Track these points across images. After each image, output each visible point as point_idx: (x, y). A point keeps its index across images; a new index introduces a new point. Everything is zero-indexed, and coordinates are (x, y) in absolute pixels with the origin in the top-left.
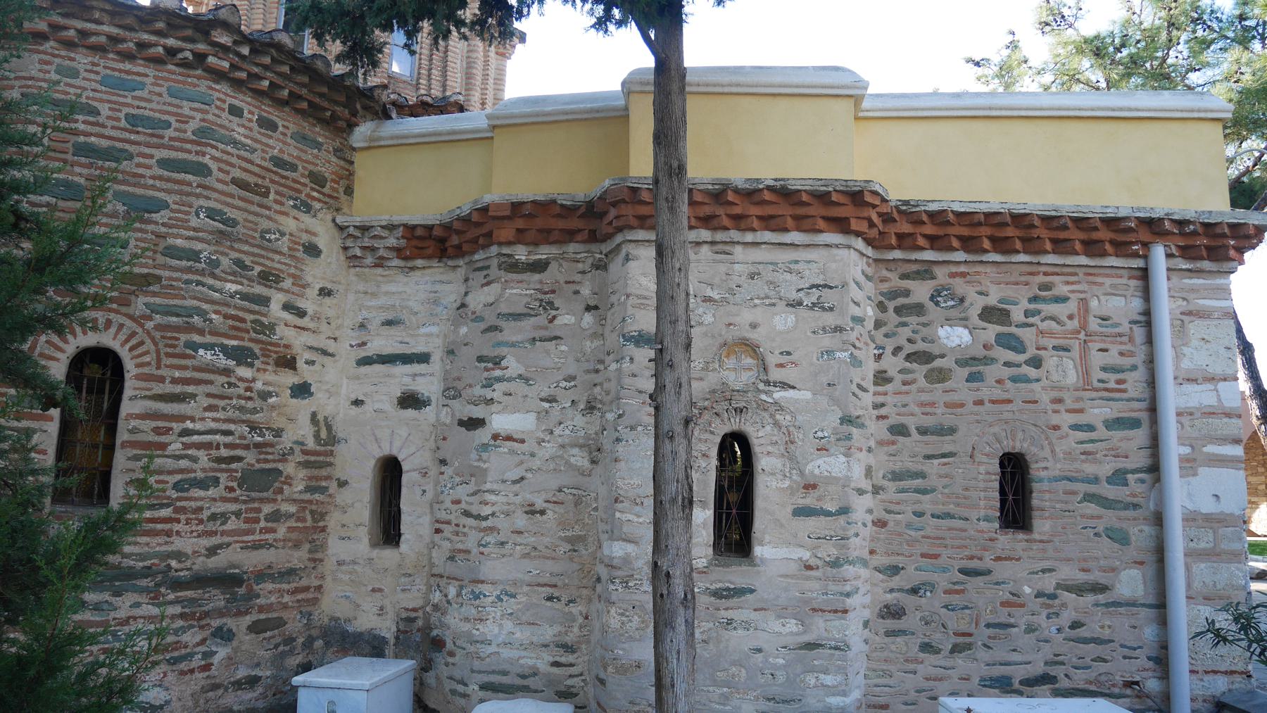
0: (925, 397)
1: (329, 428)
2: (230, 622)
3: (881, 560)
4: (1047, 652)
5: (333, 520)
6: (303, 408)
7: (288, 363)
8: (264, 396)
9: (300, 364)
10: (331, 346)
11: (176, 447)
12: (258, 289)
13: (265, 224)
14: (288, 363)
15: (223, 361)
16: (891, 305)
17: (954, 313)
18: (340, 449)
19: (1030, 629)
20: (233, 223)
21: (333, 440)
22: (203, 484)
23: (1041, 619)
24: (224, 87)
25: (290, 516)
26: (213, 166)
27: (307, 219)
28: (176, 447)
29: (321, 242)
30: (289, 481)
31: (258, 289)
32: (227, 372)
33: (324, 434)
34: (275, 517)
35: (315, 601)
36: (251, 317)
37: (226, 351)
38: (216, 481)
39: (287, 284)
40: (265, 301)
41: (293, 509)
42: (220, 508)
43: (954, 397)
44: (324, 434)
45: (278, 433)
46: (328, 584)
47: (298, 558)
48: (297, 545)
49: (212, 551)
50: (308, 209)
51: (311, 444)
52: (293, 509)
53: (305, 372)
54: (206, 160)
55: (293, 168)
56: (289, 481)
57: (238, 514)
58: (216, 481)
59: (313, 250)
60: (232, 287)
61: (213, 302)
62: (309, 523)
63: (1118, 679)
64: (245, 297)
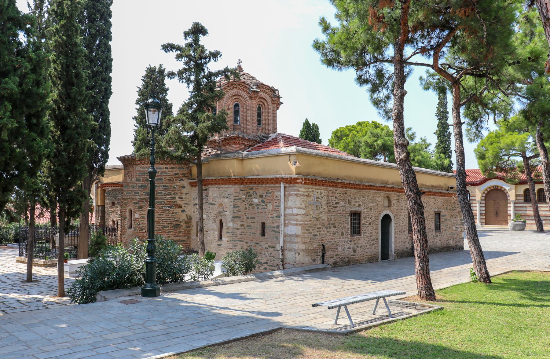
0: (251, 212)
1: (190, 217)
4: (267, 258)
5: (192, 232)
6: (184, 214)
7: (181, 207)
8: (176, 213)
9: (182, 207)
10: (189, 203)
11: (161, 222)
13: (174, 185)
14: (181, 207)
15: (168, 208)
16: (247, 195)
17: (255, 196)
18: (192, 220)
20: (168, 186)
21: (191, 218)
23: (266, 253)
24: (164, 165)
25: (182, 232)
26: (163, 178)
27: (182, 182)
28: (161, 222)
29: (185, 185)
30: (182, 226)
32: (168, 210)
33: (189, 218)
34: (180, 232)
35: (189, 245)
36: (172, 201)
37: (168, 207)
38: (168, 227)
39: (179, 194)
40: (175, 198)
41: (183, 230)
42: (169, 231)
43: (255, 212)
44: (189, 218)
45: (179, 218)
46: (191, 242)
47: (185, 238)
48: (185, 236)
50: (182, 180)
51: (186, 219)
52: (183, 230)
53: (184, 208)
54: (162, 178)
55: (178, 174)
56: (182, 226)
57: (173, 231)
58: (168, 227)
59: (184, 187)
60: (168, 197)
61: (165, 200)
62: (187, 232)
63: (276, 264)
64: (170, 198)
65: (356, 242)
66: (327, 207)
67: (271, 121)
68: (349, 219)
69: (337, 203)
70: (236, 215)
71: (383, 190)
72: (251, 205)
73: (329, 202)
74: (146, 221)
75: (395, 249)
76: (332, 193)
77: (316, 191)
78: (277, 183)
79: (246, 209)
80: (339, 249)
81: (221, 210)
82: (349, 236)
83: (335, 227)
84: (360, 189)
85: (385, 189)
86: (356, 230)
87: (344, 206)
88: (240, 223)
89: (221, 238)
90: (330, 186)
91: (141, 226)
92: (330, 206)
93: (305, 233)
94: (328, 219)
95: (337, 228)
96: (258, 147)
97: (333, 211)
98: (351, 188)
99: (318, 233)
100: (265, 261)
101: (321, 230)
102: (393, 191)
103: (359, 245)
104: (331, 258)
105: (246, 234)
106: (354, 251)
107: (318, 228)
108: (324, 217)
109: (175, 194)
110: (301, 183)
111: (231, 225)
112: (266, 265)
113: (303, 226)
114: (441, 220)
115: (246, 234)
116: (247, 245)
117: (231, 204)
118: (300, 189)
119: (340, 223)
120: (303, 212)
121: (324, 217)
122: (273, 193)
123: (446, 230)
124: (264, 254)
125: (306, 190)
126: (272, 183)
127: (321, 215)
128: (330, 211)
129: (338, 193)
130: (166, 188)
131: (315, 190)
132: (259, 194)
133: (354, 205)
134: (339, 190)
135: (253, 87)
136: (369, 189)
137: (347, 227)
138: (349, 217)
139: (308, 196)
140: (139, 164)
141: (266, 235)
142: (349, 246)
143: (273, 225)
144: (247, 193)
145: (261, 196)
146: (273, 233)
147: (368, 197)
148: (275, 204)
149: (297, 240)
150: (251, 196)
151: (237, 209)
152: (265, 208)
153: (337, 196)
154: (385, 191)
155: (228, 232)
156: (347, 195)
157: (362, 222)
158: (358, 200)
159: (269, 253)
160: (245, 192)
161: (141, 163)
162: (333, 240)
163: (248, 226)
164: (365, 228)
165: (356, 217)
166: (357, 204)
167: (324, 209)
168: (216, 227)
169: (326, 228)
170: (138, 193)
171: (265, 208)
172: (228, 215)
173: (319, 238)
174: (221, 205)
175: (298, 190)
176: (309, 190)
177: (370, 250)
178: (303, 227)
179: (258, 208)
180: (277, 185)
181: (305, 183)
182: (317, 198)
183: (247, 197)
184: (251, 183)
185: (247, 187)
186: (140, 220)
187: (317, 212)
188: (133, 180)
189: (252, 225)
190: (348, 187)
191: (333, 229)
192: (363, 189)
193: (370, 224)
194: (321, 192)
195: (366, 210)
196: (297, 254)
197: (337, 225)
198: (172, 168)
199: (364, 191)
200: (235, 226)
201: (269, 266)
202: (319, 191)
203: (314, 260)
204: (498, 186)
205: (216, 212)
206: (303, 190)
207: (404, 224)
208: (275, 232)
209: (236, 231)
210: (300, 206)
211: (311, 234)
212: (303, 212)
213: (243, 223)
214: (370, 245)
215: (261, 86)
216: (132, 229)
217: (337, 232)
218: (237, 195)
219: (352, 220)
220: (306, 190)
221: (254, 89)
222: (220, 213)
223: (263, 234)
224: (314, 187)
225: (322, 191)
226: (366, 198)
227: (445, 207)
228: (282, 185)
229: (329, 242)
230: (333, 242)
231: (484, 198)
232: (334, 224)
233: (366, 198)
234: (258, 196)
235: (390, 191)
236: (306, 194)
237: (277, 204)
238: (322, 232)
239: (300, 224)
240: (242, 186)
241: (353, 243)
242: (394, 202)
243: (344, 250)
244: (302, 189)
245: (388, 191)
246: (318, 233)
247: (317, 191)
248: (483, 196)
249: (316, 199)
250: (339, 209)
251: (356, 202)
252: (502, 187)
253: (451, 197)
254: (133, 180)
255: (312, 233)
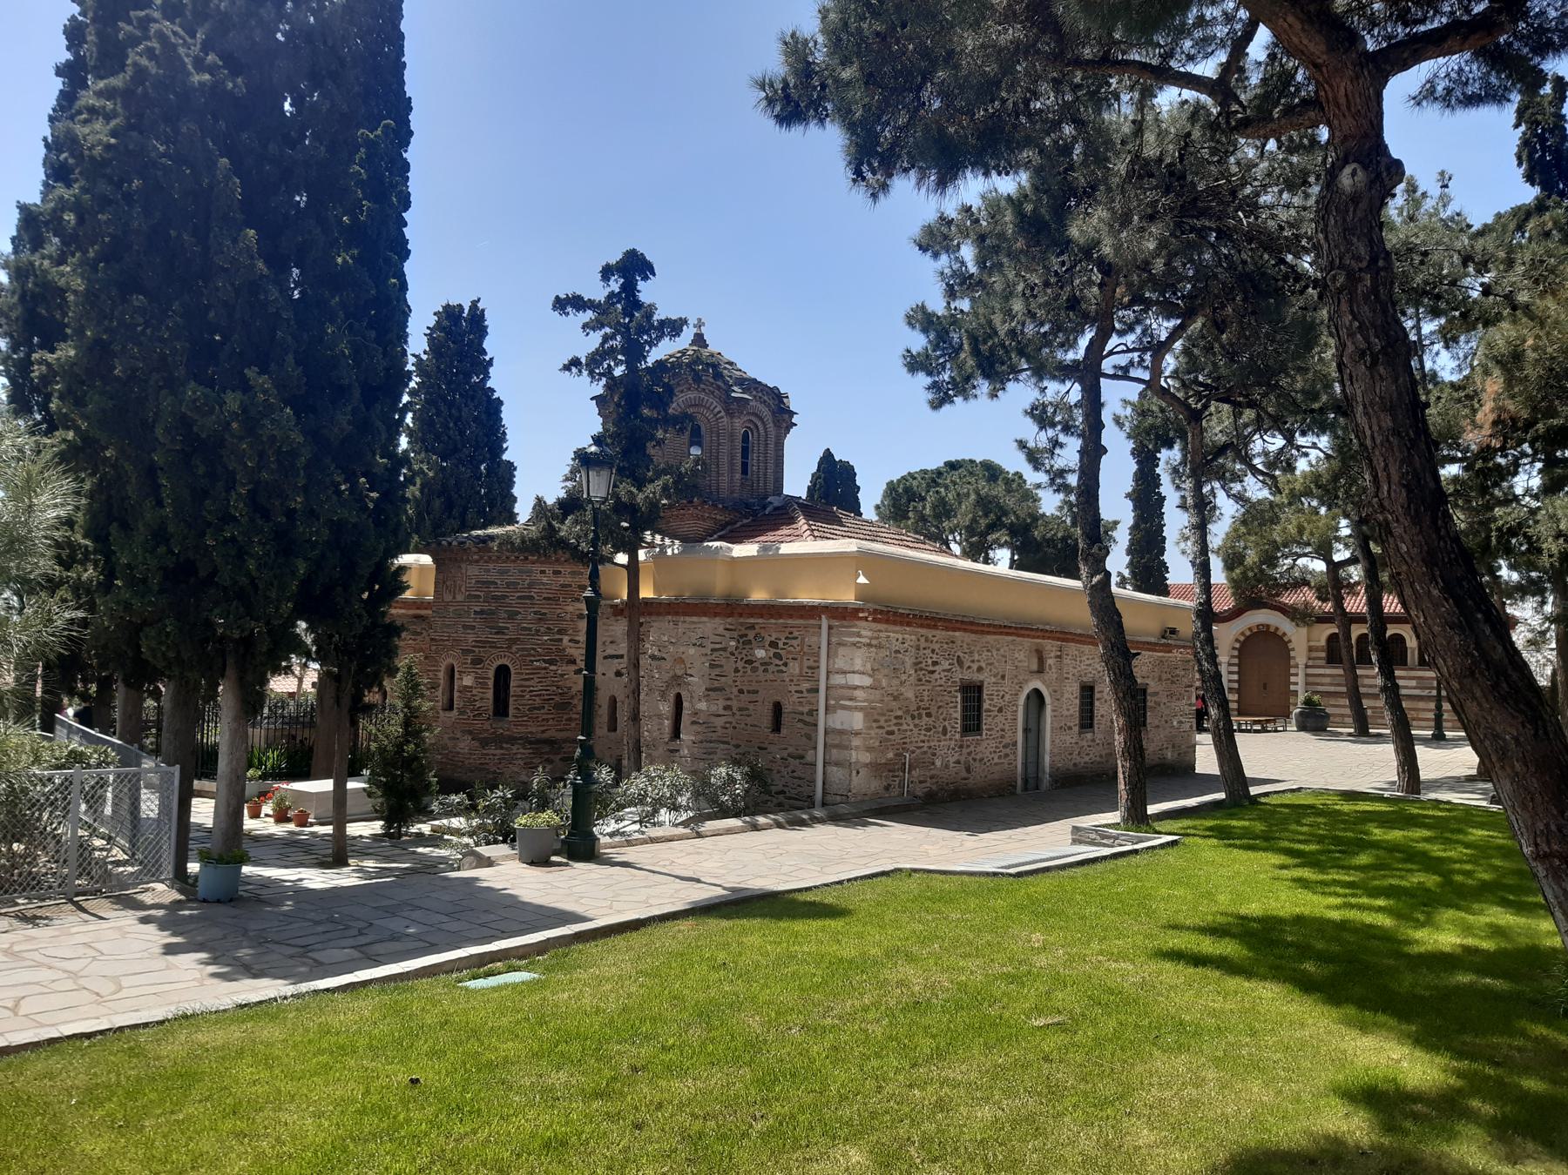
2: (552, 757)
3: (734, 742)
7: (574, 662)
8: (562, 675)
12: (558, 637)
14: (574, 662)
19: (779, 772)
20: (545, 614)
22: (538, 709)
30: (575, 706)
31: (558, 637)
32: (545, 668)
34: (570, 719)
37: (544, 661)
40: (561, 640)
45: (570, 688)
49: (543, 732)
56: (575, 706)
65: (972, 748)
67: (771, 465)
68: (959, 699)
69: (935, 663)
70: (716, 684)
71: (1028, 636)
72: (749, 662)
74: (490, 694)
75: (1051, 767)
76: (926, 640)
77: (896, 636)
78: (812, 617)
79: (737, 670)
80: (938, 763)
81: (680, 673)
82: (958, 736)
83: (929, 715)
84: (982, 632)
85: (1033, 633)
86: (972, 722)
87: (949, 670)
88: (721, 703)
89: (676, 733)
90: (922, 626)
91: (478, 704)
92: (921, 669)
93: (870, 728)
96: (743, 526)
98: (965, 630)
99: (895, 728)
100: (780, 788)
101: (903, 721)
102: (1049, 638)
103: (978, 757)
104: (921, 782)
105: (735, 728)
106: (968, 770)
107: (896, 717)
108: (910, 694)
109: (561, 632)
110: (866, 619)
111: (702, 706)
112: (781, 797)
113: (868, 712)
114: (1148, 704)
115: (735, 728)
116: (740, 750)
117: (704, 659)
118: (863, 633)
119: (939, 707)
120: (867, 681)
121: (910, 694)
122: (803, 639)
123: (1158, 727)
124: (779, 772)
125: (875, 635)
126: (802, 617)
128: (920, 680)
130: (542, 618)
132: (768, 639)
133: (969, 667)
134: (940, 634)
135: (735, 388)
136: (1001, 633)
137: (955, 715)
138: (959, 695)
139: (879, 647)
140: (477, 561)
141: (784, 731)
142: (956, 756)
143: (801, 709)
144: (741, 636)
145: (774, 644)
146: (800, 725)
147: (998, 650)
148: (806, 663)
149: (856, 742)
150: (750, 642)
151: (717, 671)
152: (782, 672)
153: (936, 647)
154: (1034, 637)
155: (694, 723)
157: (986, 706)
158: (976, 657)
159: (789, 769)
160: (735, 634)
161: (481, 558)
162: (926, 744)
163: (740, 709)
164: (990, 719)
165: (972, 694)
166: (975, 666)
168: (666, 708)
169: (913, 717)
170: (473, 628)
171: (782, 672)
172: (697, 682)
173: (896, 737)
174: (681, 661)
175: (859, 635)
177: (998, 768)
178: (866, 716)
179: (765, 671)
180: (812, 622)
181: (874, 620)
182: (897, 652)
183: (740, 645)
184: (751, 615)
185: (742, 624)
186: (474, 692)
187: (895, 682)
188: (460, 598)
189: (751, 707)
190: (959, 630)
192: (989, 633)
193: (1000, 710)
195: (993, 680)
196: (854, 773)
197: (933, 710)
198: (557, 573)
199: (990, 638)
200: (714, 708)
201: (790, 798)
202: (900, 637)
204: (1268, 626)
205: (666, 677)
206: (869, 634)
207: (1071, 712)
208: (806, 723)
209: (713, 719)
211: (881, 731)
212: (867, 681)
213: (729, 703)
214: (1000, 757)
215: (752, 385)
216: (455, 712)
218: (718, 639)
219: (964, 700)
221: (737, 393)
222: (677, 680)
223: (777, 726)
224: (891, 627)
226: (995, 653)
227: (1156, 675)
228: (825, 622)
230: (925, 749)
231: (1236, 653)
233: (995, 653)
234: (767, 644)
235: (1044, 638)
236: (874, 642)
237: (811, 663)
238: (905, 727)
239: (861, 709)
240: (729, 620)
241: (965, 751)
242: (1050, 661)
243: (947, 766)
244: (866, 630)
245: (1038, 637)
246: (895, 728)
247: (897, 636)
248: (1234, 648)
250: (939, 676)
251: (973, 661)
252: (1277, 629)
253: (1170, 652)
254: (460, 598)
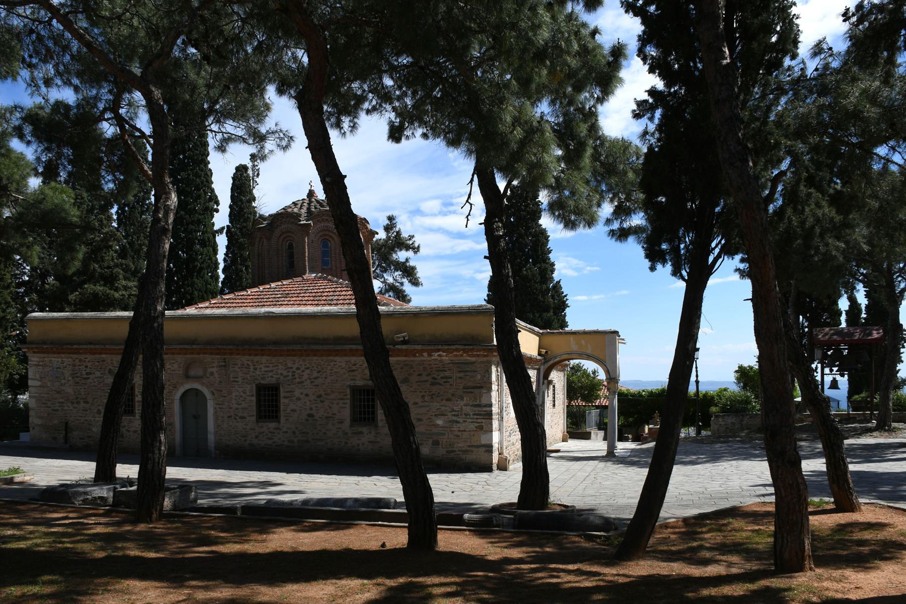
66: (73, 378)
73: (75, 372)
83: (87, 402)
87: (100, 378)
92: (77, 377)
94: (75, 392)
95: (89, 404)
97: (83, 383)
99: (60, 408)
101: (65, 405)
107: (59, 402)
119: (94, 398)
121: (70, 390)
125: (42, 359)
127: (63, 388)
129: (89, 361)
131: (53, 359)
139: (45, 366)
153: (89, 365)
156: (105, 363)
167: (69, 380)
169: (72, 403)
176: (45, 359)
191: (82, 405)
194: (62, 361)
202: (60, 360)
203: (54, 438)
210: (33, 377)
217: (91, 409)
220: (42, 359)
225: (64, 359)
229: (77, 420)
230: (82, 421)
232: (86, 399)
236: (41, 363)
238: (66, 408)
247: (57, 359)
249: (55, 370)
255: (50, 407)
